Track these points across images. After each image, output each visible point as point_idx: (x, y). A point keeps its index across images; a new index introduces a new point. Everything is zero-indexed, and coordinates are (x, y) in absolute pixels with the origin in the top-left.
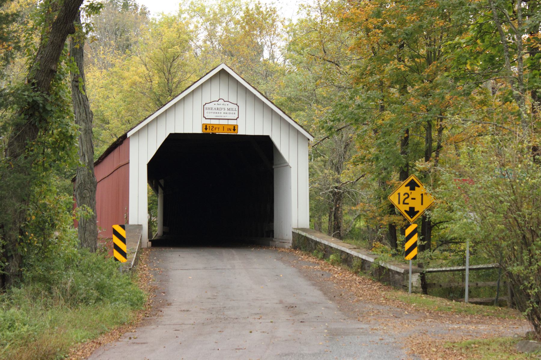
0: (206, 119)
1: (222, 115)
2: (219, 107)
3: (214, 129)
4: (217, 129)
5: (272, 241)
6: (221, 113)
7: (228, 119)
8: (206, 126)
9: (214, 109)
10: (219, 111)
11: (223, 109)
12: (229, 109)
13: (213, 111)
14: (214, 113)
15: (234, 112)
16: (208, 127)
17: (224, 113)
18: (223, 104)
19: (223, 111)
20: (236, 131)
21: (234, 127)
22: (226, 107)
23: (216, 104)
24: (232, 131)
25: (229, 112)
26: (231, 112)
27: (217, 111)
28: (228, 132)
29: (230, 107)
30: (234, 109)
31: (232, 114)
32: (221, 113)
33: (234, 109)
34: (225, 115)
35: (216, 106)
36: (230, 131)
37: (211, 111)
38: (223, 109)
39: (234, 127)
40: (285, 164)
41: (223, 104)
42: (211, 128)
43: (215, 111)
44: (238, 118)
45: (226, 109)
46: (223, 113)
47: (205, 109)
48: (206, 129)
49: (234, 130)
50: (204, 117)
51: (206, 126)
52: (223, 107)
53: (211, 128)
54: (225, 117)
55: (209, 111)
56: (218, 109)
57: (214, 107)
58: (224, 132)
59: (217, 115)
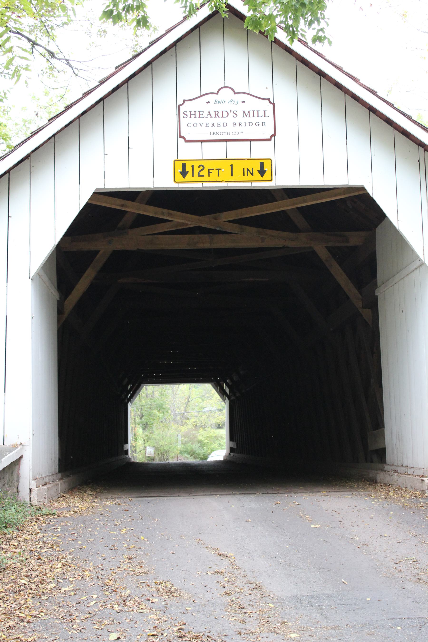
0: (186, 141)
1: (230, 128)
2: (219, 108)
3: (205, 172)
4: (215, 172)
5: (383, 470)
6: (225, 125)
7: (250, 140)
8: (184, 166)
9: (205, 114)
10: (221, 120)
11: (231, 115)
12: (246, 114)
13: (203, 121)
14: (207, 125)
15: (260, 120)
16: (189, 168)
17: (235, 124)
18: (231, 101)
19: (230, 120)
20: (267, 176)
21: (262, 164)
22: (240, 108)
23: (212, 102)
24: (257, 176)
25: (247, 120)
26: (254, 120)
27: (216, 120)
28: (246, 178)
29: (251, 110)
30: (261, 113)
31: (257, 125)
32: (225, 125)
33: (261, 113)
34: (238, 129)
35: (213, 108)
36: (250, 177)
37: (198, 120)
38: (231, 115)
39: (262, 164)
40: (418, 263)
41: (231, 101)
42: (197, 170)
43: (210, 120)
44: (274, 135)
45: (240, 114)
46: (230, 125)
47: (182, 115)
48: (184, 173)
49: (262, 172)
50: (181, 137)
51: (184, 166)
52: (233, 107)
53: (197, 170)
54: (237, 133)
55: (193, 120)
56: (216, 114)
57: (206, 108)
58: (233, 179)
59: (216, 129)
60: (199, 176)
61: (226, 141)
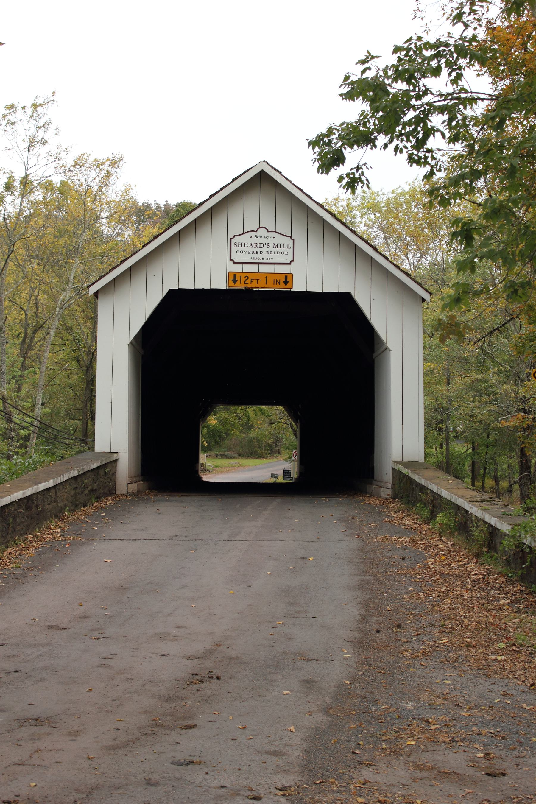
0: (235, 263)
1: (264, 255)
2: (258, 241)
3: (248, 281)
6: (261, 252)
8: (235, 276)
9: (249, 245)
10: (259, 250)
11: (266, 246)
12: (275, 246)
13: (247, 249)
15: (285, 250)
16: (238, 278)
17: (268, 252)
18: (266, 237)
19: (265, 249)
20: (289, 285)
21: (286, 277)
22: (271, 242)
23: (253, 237)
24: (282, 284)
25: (276, 250)
26: (281, 250)
27: (255, 249)
28: (275, 286)
30: (286, 246)
31: (282, 253)
32: (261, 252)
33: (286, 246)
34: (269, 256)
35: (254, 241)
36: (278, 285)
37: (244, 249)
38: (266, 246)
39: (286, 277)
41: (266, 237)
42: (243, 279)
43: (251, 249)
44: (293, 261)
45: (272, 246)
46: (265, 252)
47: (233, 245)
48: (235, 281)
49: (286, 282)
50: (231, 260)
51: (235, 276)
54: (269, 259)
55: (240, 249)
58: (266, 286)
59: (255, 255)
60: (245, 283)
61: (259, 263)
